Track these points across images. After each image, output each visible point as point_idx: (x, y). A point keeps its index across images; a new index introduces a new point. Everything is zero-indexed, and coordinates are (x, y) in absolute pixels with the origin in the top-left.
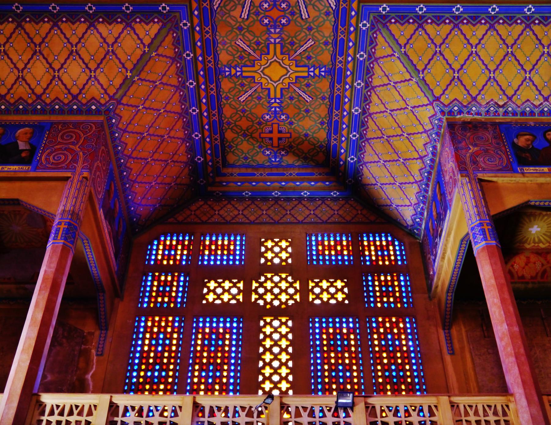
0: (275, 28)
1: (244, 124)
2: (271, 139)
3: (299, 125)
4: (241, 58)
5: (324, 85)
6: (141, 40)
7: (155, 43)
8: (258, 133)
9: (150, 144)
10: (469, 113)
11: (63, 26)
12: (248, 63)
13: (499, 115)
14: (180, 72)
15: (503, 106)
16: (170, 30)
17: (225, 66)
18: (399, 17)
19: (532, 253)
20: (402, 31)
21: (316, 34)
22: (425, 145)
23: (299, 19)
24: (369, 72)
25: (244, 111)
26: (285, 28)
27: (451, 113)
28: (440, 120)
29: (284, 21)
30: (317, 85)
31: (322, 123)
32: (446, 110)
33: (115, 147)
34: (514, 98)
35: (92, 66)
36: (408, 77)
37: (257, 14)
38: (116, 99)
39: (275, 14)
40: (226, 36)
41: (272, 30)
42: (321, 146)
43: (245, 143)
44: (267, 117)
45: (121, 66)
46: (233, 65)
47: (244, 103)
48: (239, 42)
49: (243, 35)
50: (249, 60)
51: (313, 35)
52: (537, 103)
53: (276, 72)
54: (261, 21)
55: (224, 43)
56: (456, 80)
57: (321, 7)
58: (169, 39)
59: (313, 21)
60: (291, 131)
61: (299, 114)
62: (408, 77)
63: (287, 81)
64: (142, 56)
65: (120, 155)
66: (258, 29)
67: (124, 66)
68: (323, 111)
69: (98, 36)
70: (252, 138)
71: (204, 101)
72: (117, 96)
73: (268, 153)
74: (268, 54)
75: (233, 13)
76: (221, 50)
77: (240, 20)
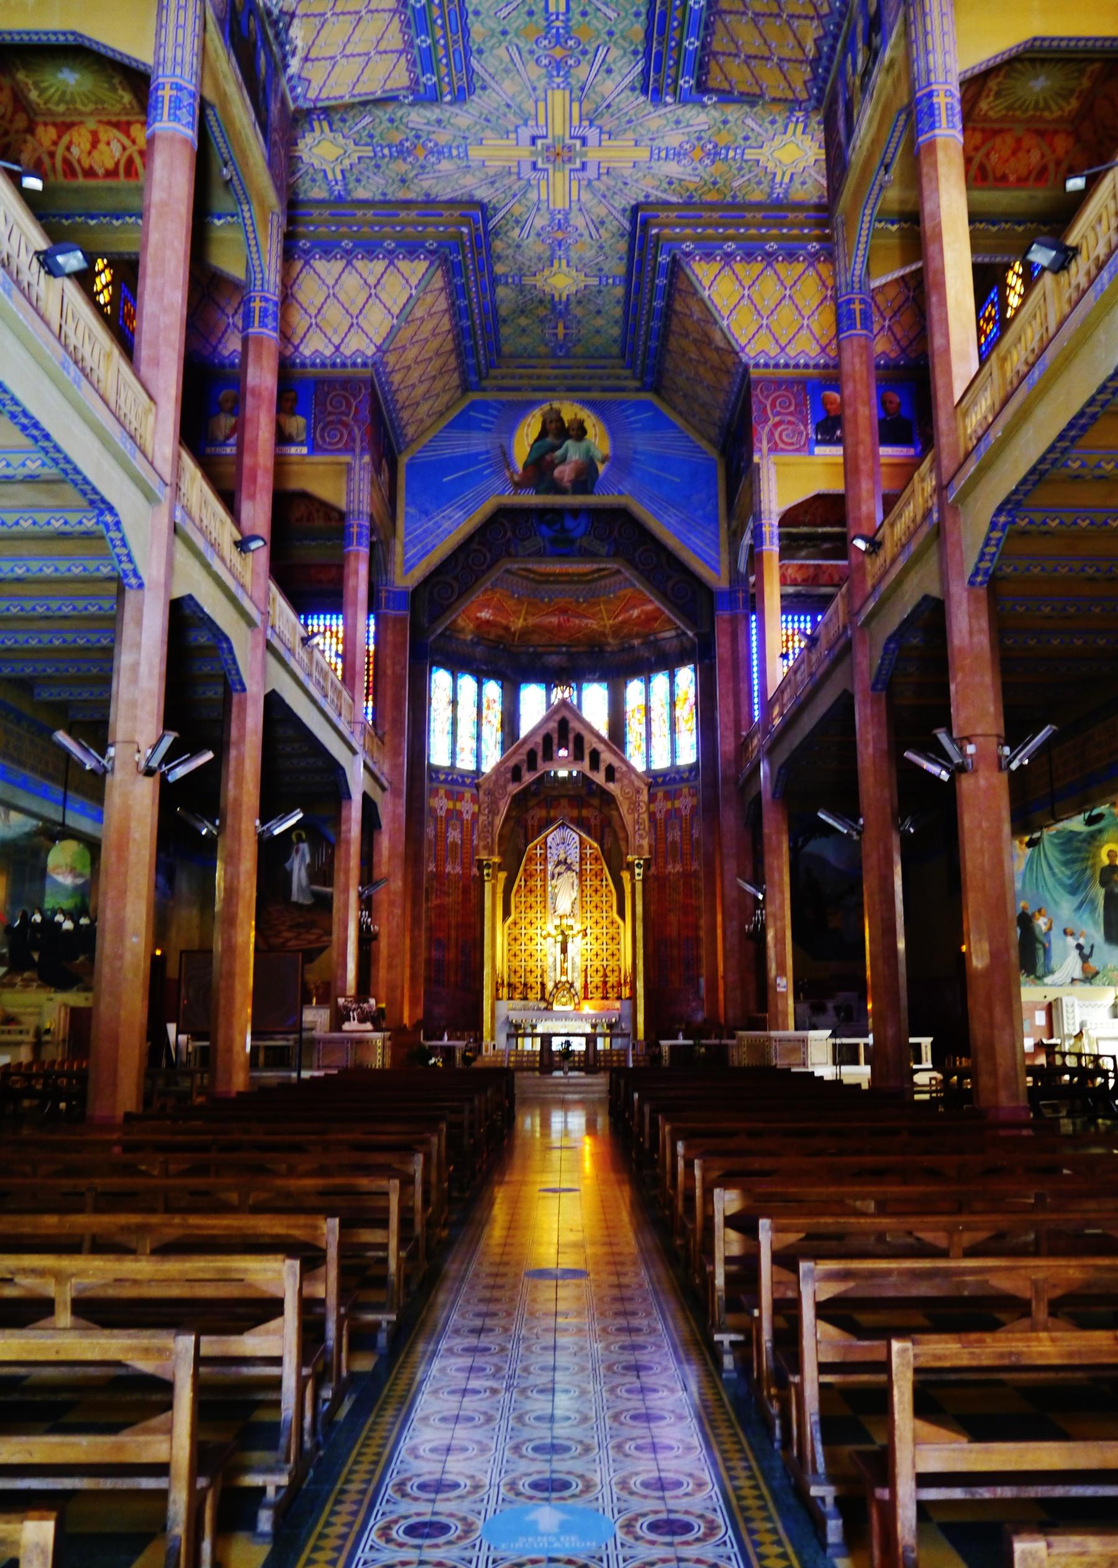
19: (12, 89)
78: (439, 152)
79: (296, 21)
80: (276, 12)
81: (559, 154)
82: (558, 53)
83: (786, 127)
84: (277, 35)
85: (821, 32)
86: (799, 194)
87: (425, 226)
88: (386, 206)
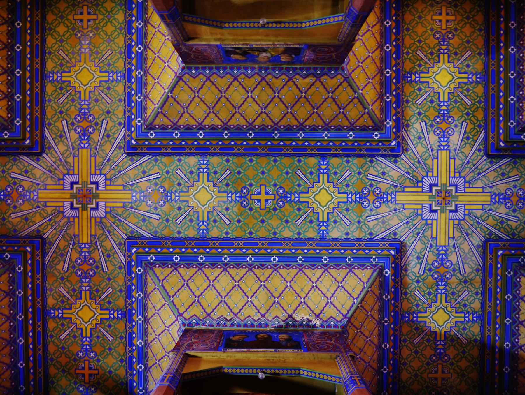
0: (86, 278)
1: (63, 360)
3: (104, 363)
4: (62, 302)
10: (203, 325)
12: (67, 307)
13: (226, 326)
15: (230, 320)
21: (113, 284)
23: (101, 272)
25: (63, 348)
26: (92, 279)
27: (190, 324)
29: (91, 273)
30: (116, 326)
31: (122, 361)
32: (187, 322)
34: (239, 315)
37: (74, 267)
39: (85, 267)
41: (84, 280)
42: (122, 383)
43: (64, 378)
44: (81, 354)
46: (57, 308)
48: (61, 289)
49: (64, 284)
51: (111, 284)
52: (256, 318)
53: (86, 314)
54: (76, 273)
55: (51, 290)
57: (116, 263)
59: (111, 274)
60: (98, 367)
61: (104, 351)
63: (94, 322)
68: (121, 350)
70: (70, 374)
73: (81, 389)
74: (81, 299)
75: (57, 267)
78: (442, 260)
79: (294, 316)
80: (282, 323)
81: (444, 198)
82: (371, 198)
83: (423, 82)
84: (294, 326)
85: (297, 76)
86: (478, 65)
87: (497, 275)
88: (486, 294)
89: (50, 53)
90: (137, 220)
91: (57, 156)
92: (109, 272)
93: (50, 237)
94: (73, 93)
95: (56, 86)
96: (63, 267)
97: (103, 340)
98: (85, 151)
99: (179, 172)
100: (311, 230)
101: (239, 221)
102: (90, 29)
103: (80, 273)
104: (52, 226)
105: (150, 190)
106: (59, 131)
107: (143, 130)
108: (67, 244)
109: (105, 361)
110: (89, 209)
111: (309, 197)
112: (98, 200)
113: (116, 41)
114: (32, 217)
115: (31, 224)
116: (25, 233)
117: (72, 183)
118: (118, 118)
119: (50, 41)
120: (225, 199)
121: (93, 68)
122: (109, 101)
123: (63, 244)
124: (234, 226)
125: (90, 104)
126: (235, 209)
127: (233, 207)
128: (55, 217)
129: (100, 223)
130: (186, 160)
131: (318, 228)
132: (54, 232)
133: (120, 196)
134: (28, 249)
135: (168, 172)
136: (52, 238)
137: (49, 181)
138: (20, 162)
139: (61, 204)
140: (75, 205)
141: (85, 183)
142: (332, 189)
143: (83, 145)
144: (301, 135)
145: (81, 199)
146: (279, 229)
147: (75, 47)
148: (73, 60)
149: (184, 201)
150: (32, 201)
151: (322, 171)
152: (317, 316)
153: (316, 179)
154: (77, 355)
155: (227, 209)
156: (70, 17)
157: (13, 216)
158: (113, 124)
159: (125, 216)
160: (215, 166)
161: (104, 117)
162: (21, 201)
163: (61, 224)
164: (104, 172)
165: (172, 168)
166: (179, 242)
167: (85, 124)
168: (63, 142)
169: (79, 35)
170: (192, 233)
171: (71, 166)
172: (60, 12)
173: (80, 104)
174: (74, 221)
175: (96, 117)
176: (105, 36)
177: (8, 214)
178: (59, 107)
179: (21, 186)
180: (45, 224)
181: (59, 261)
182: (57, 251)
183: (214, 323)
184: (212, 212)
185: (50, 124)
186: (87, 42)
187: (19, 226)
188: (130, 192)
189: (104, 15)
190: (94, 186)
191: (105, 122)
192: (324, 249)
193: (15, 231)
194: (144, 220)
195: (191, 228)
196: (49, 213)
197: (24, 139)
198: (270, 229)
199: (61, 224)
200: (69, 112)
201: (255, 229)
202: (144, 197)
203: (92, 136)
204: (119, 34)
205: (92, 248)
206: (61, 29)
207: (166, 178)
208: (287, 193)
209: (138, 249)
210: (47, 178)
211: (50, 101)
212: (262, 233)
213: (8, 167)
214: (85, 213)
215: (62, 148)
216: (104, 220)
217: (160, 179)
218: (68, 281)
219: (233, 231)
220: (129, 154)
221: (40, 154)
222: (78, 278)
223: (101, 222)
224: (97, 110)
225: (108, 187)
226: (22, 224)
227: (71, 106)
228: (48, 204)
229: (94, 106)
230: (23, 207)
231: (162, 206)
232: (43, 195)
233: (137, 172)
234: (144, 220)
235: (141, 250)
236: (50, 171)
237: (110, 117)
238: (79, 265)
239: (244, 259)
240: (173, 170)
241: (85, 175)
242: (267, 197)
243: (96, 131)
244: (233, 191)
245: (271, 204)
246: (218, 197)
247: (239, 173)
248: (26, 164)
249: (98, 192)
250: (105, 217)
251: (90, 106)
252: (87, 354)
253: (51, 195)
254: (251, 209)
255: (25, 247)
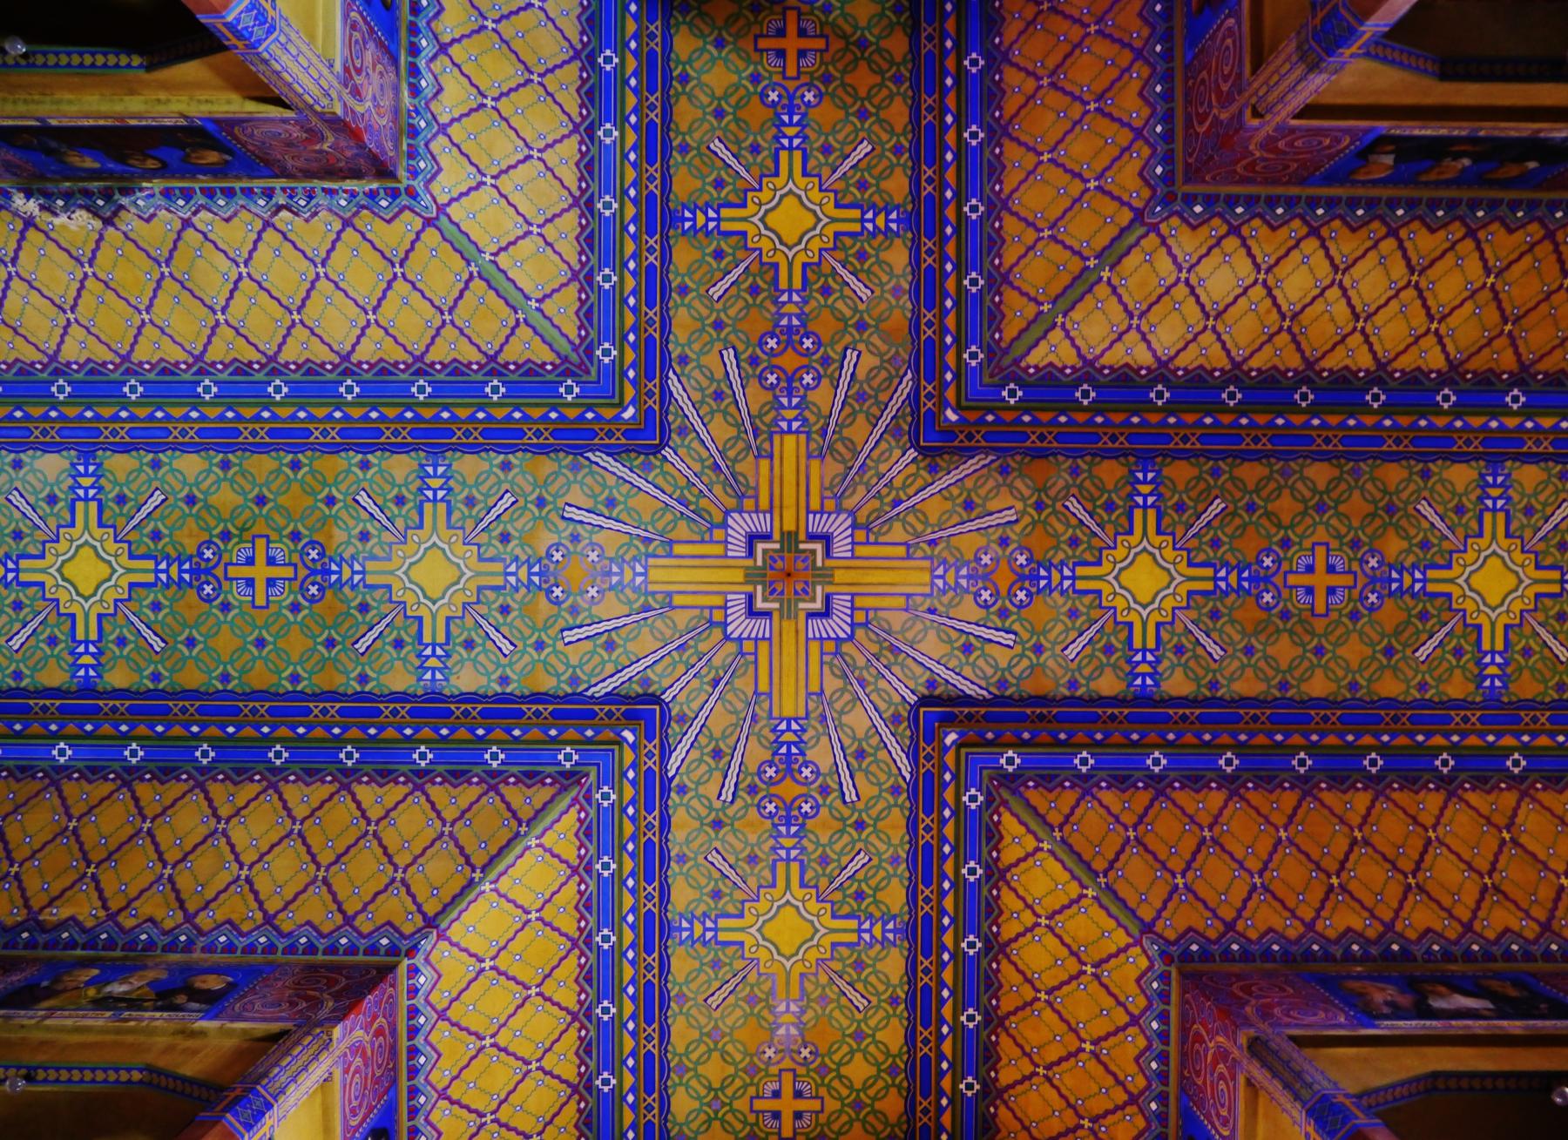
0: (790, 327)
1: (864, 79)
2: (802, 33)
3: (738, 72)
4: (862, 256)
5: (685, 184)
6: (1068, 335)
7: (1039, 327)
8: (833, 49)
9: (1086, 73)
10: (353, 194)
11: (1224, 363)
12: (848, 241)
13: (284, 190)
14: (996, 242)
15: (280, 208)
16: (1006, 351)
17: (897, 234)
18: (537, 374)
20: (525, 348)
21: (705, 312)
22: (440, 90)
23: (740, 347)
24: (587, 240)
25: (863, 115)
26: (769, 326)
27: (394, 194)
28: (414, 173)
29: (772, 343)
30: (698, 184)
31: (684, 79)
32: (404, 200)
33: (1167, 96)
34: (259, 224)
35: (1181, 291)
36: (503, 260)
37: (826, 360)
38: (1143, 224)
39: (789, 361)
40: (891, 308)
41: (795, 322)
42: (685, 10)
43: (863, 24)
44: (809, 96)
45: (1120, 290)
46: (881, 238)
47: (862, 135)
48: (864, 293)
49: (855, 310)
50: (845, 249)
51: (712, 309)
52: (204, 215)
53: (790, 219)
54: (818, 343)
55: (897, 291)
56: (398, 263)
57: (696, 373)
58: (1010, 331)
59: (712, 342)
60: (755, 56)
61: (737, 107)
62: (503, 260)
63: (765, 195)
64: (1072, 308)
65: (1161, 67)
66: (824, 326)
67: (1114, 290)
68: (684, 113)
69: (1155, 345)
70: (845, 37)
71: (949, 230)
72: (1141, 231)
74: (805, 265)
75: (875, 361)
76: (900, 1055)
77: (861, 347)
79: (98, 224)
80: (124, 201)
84: (87, 193)
89: (894, 1001)
90: (632, 503)
91: (874, 697)
92: (718, 346)
93: (897, 453)
94: (823, 882)
95: (876, 902)
96: (864, 362)
97: (738, 142)
98: (788, 711)
99: (506, 647)
100: (121, 477)
101: (330, 501)
102: (774, 1070)
103: (808, 343)
104: (889, 484)
105: (593, 592)
106: (867, 772)
107: (593, 771)
108: (846, 432)
109: (735, 78)
110: (776, 536)
111: (129, 571)
112: (749, 562)
113: (695, 1034)
114: (952, 512)
115: (955, 491)
116: (973, 464)
117: (826, 613)
118: (688, 807)
119: (893, 1036)
120: (370, 566)
121: (763, 955)
122: (715, 858)
123: (858, 431)
124: (343, 487)
125: (774, 849)
126: (340, 538)
127: (348, 543)
128: (879, 513)
129: (742, 494)
130: (484, 681)
131: (103, 481)
132: (883, 468)
133: (683, 575)
134: (951, 416)
135: (540, 646)
136: (891, 450)
137: (897, 620)
138: (985, 678)
139: (862, 551)
140: (818, 547)
141: (788, 613)
142: (63, 596)
143: (794, 726)
144: (134, 753)
145: (800, 565)
146: (212, 477)
147: (817, 1017)
148: (823, 979)
149: (491, 560)
150: (951, 560)
151: (92, 649)
152: (29, 223)
153: (107, 626)
154: (820, 96)
155: (364, 536)
156: (832, 1105)
157: (1010, 516)
158: (701, 790)
159: (669, 517)
160: (398, 664)
161: (731, 811)
162: (986, 559)
163: (861, 490)
164: (731, 647)
165: (527, 659)
166: (501, 438)
167: (789, 789)
168: (854, 738)
169: (805, 1053)
170: (467, 466)
171: (831, 665)
172: (864, 1122)
173: (803, 849)
174: (823, 499)
175: (753, 812)
176: (729, 1048)
177: (1027, 520)
178: (866, 841)
179: (986, 606)
180: (911, 491)
181: (869, 379)
182: (875, 411)
183: (321, 199)
184: (408, 528)
185: (895, 790)
186: (782, 1031)
187: (991, 484)
188: (651, 588)
189: (732, 1111)
190: (760, 604)
191: (727, 794)
192: (70, 420)
193: (1004, 471)
194: (611, 503)
195: (471, 481)
196: (897, 525)
197: (959, 745)
198: (240, 479)
199: (861, 490)
200: (837, 825)
201: (281, 478)
202: (609, 573)
203: (767, 756)
204: (687, 1054)
205: (767, 419)
206: (859, 1071)
207: (545, 628)
208: (190, 585)
209: (618, 417)
210: (904, 630)
211: (895, 860)
212: (263, 465)
213: (1025, 663)
214: (789, 526)
215: (858, 720)
216: (731, 502)
217: (561, 624)
218: (842, 319)
219: (348, 471)
220: (655, 699)
221: (924, 701)
222: (812, 327)
223: (741, 497)
224: (752, 831)
225: (718, 601)
226: (982, 492)
227: (831, 843)
228: (901, 551)
229: (758, 844)
230: (981, 541)
231: (557, 546)
232: (916, 578)
233: (631, 646)
234: (611, 503)
235: (608, 413)
236: (895, 650)
237: (711, 809)
238: (807, 368)
239: (297, 390)
240: (524, 652)
241: (789, 638)
242: (246, 572)
243: (753, 768)
244: (346, 589)
245: (235, 551)
246: (392, 573)
247: (330, 643)
248: (967, 671)
249: (749, 588)
250: (727, 513)
251: (772, 842)
252: (791, 97)
253: (890, 579)
254: (295, 536)
255: (962, 420)
